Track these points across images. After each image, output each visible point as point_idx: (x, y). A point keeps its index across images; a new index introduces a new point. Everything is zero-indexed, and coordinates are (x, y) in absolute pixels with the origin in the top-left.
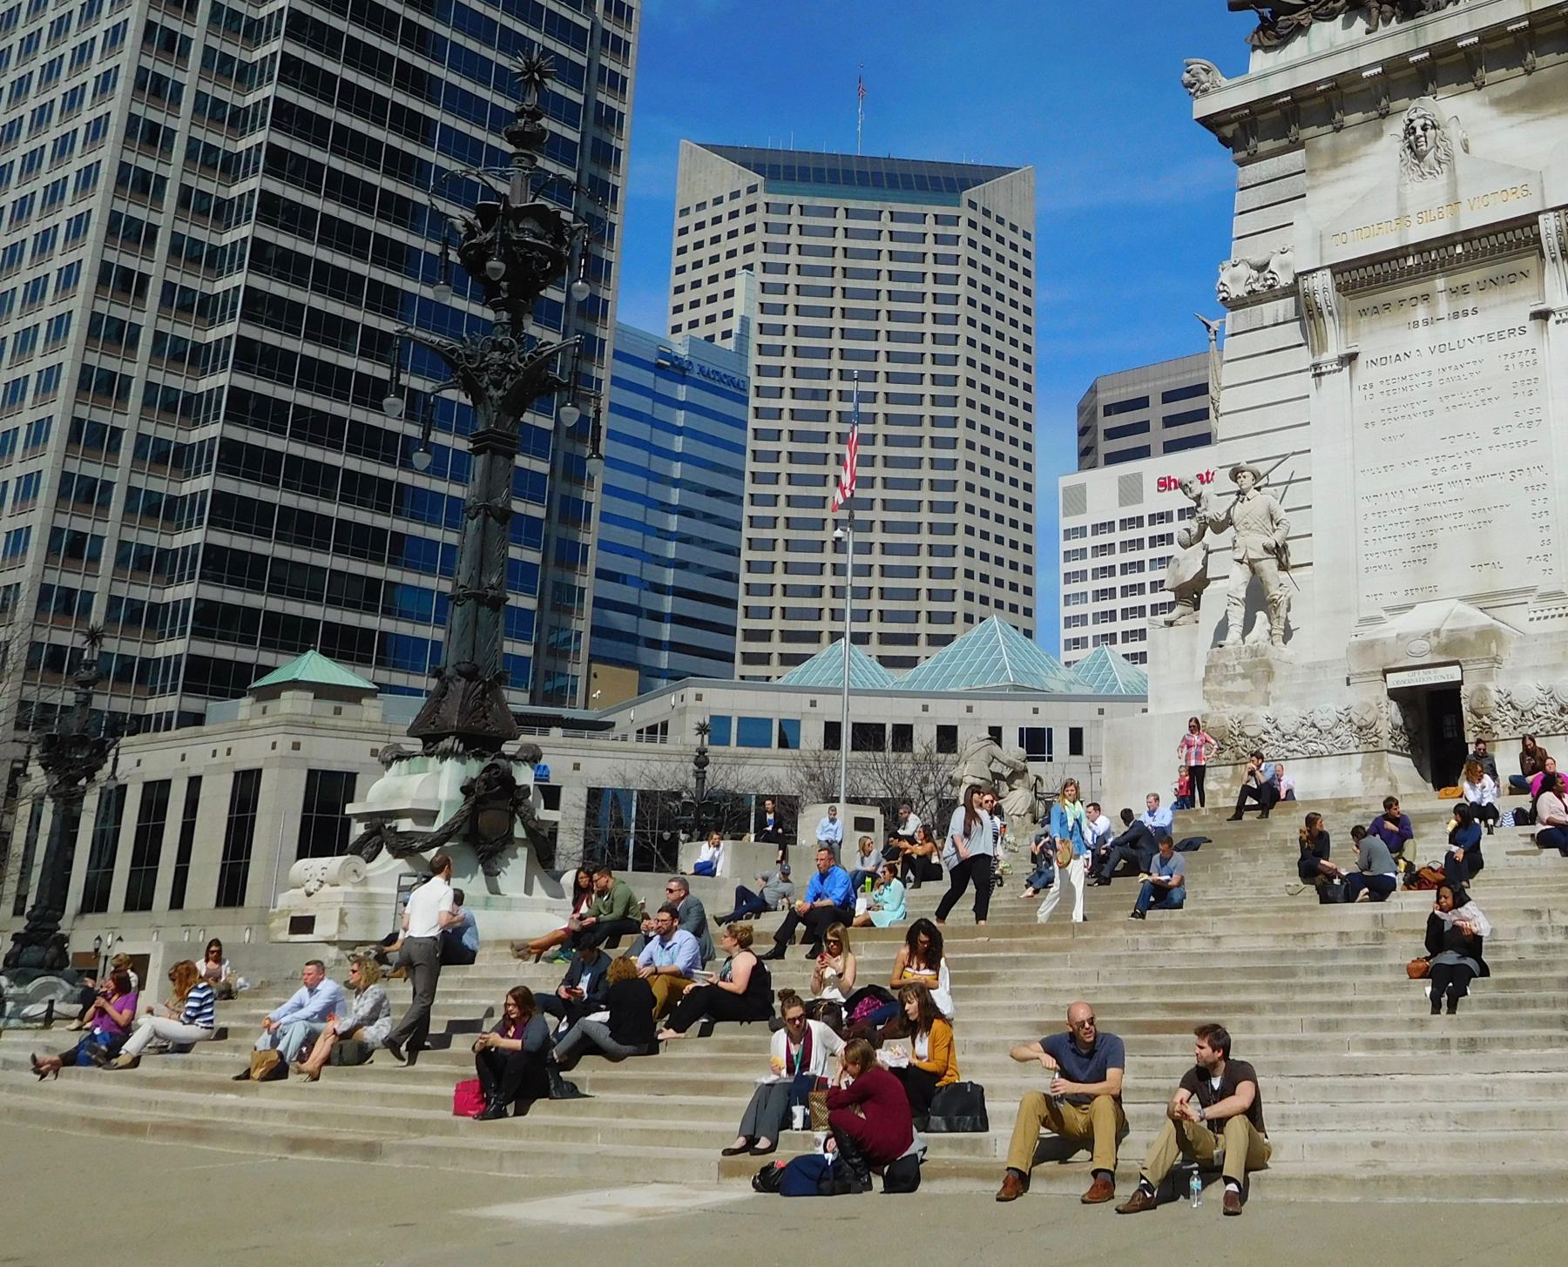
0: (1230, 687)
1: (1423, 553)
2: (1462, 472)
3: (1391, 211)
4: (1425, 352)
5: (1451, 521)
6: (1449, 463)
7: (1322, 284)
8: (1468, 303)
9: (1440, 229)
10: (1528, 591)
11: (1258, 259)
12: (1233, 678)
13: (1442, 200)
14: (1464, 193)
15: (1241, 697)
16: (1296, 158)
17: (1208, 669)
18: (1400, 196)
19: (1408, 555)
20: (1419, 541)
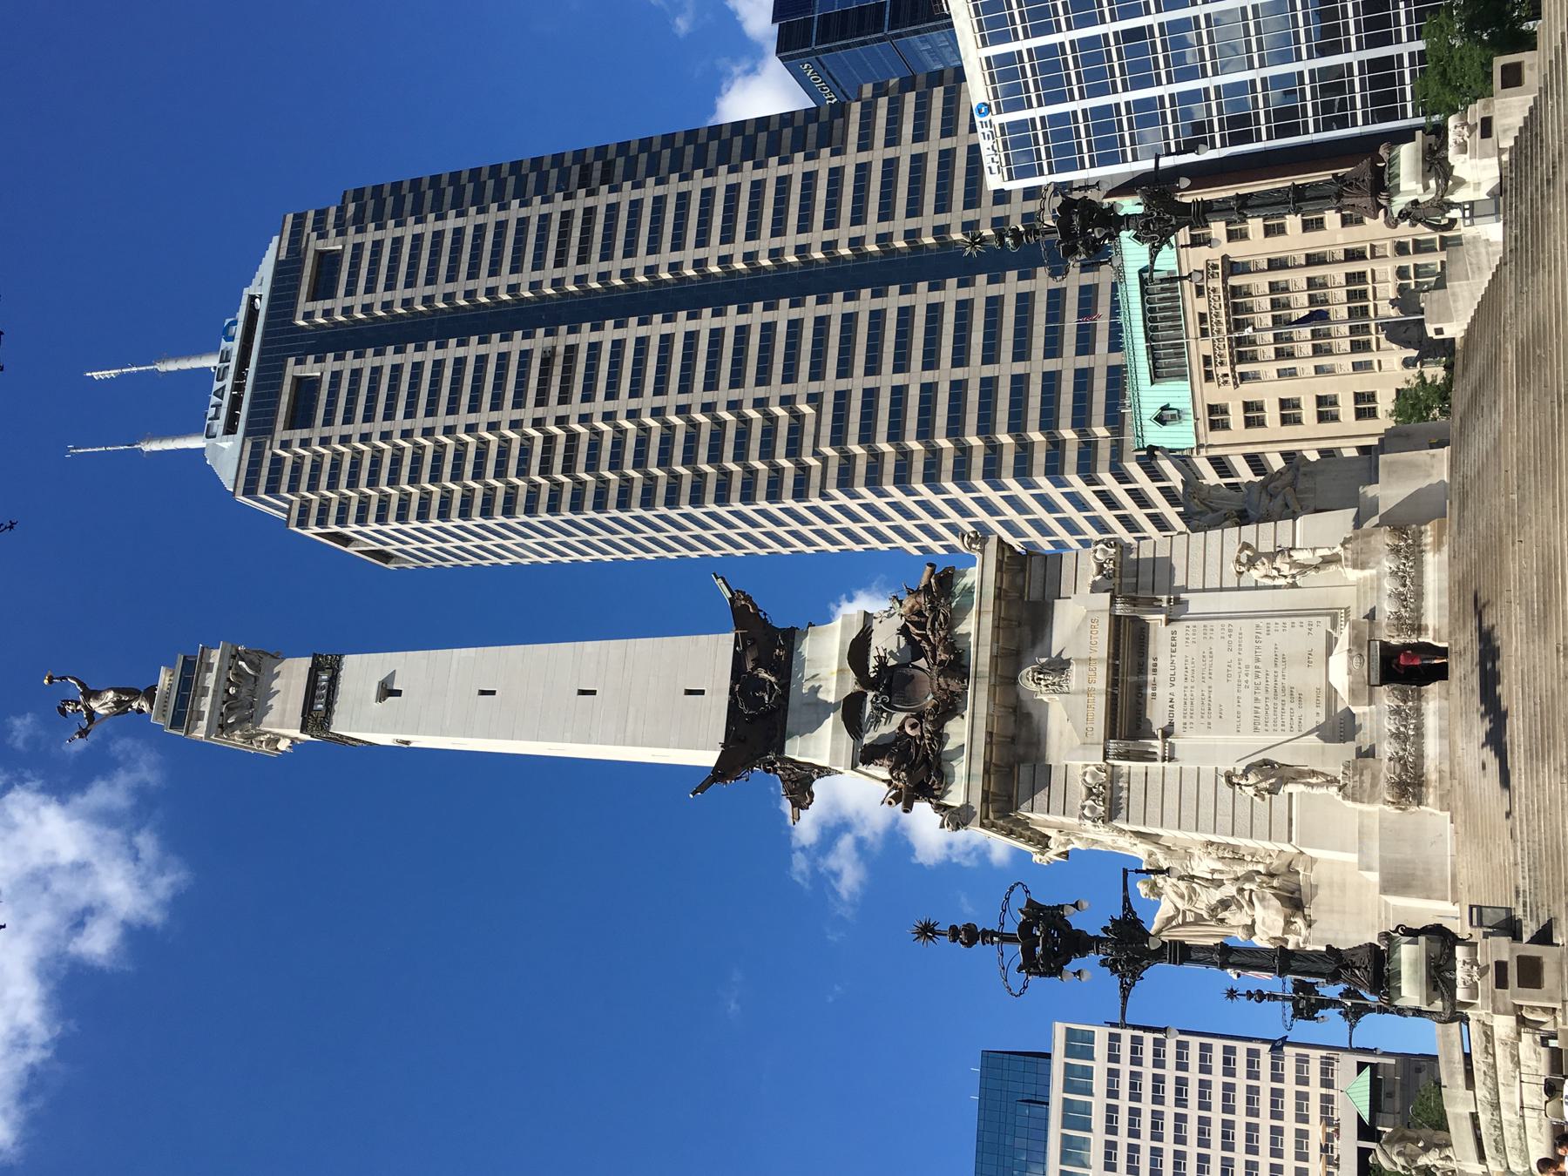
0: (1367, 785)
1: (1296, 695)
2: (1252, 671)
3: (1082, 699)
4: (1172, 690)
5: (1279, 678)
6: (1244, 678)
7: (1112, 744)
8: (1151, 662)
9: (1102, 672)
10: (1329, 635)
11: (1084, 791)
12: (1362, 782)
13: (1085, 668)
14: (1085, 656)
15: (1375, 778)
16: (1024, 771)
17: (1354, 800)
18: (1075, 693)
19: (1295, 705)
20: (1287, 699)
